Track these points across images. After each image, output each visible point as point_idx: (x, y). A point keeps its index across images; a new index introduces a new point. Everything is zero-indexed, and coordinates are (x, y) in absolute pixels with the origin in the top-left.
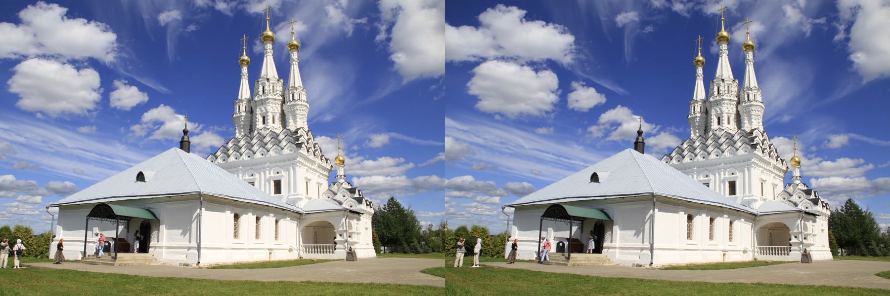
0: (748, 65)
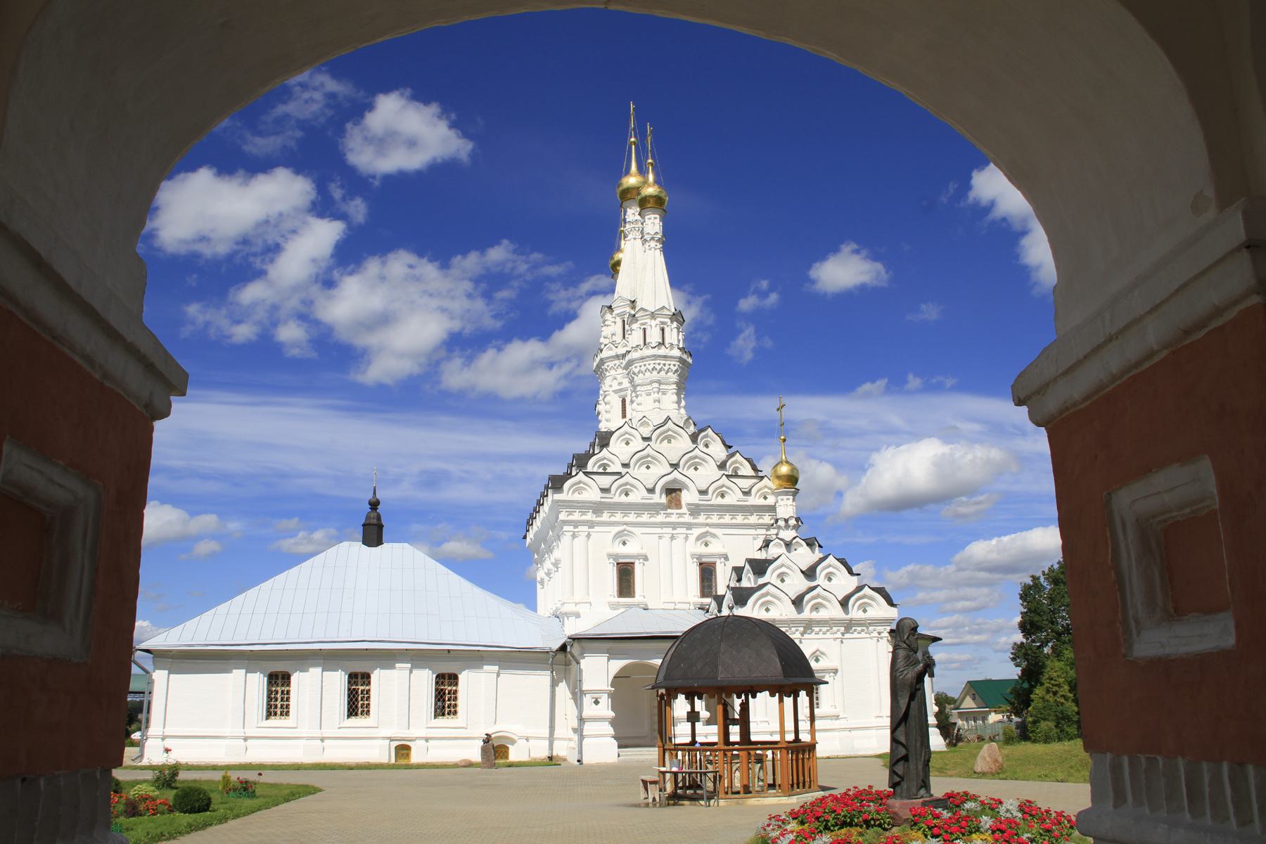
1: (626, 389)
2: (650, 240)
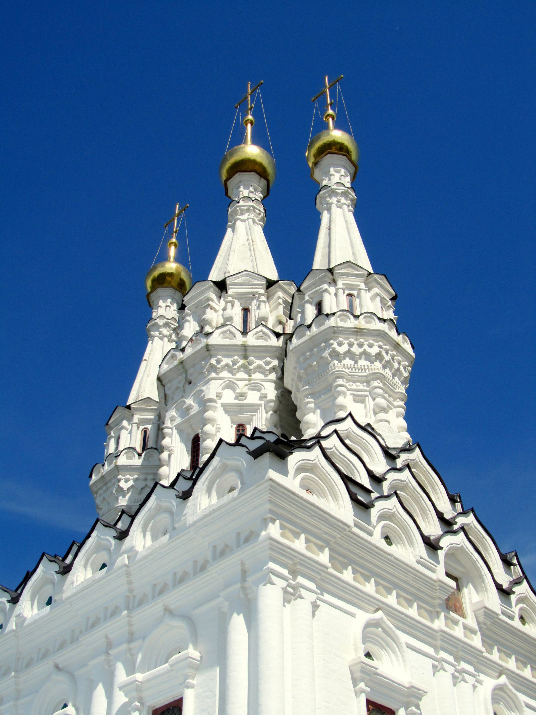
0: (329, 210)
1: (254, 408)
2: (342, 193)
